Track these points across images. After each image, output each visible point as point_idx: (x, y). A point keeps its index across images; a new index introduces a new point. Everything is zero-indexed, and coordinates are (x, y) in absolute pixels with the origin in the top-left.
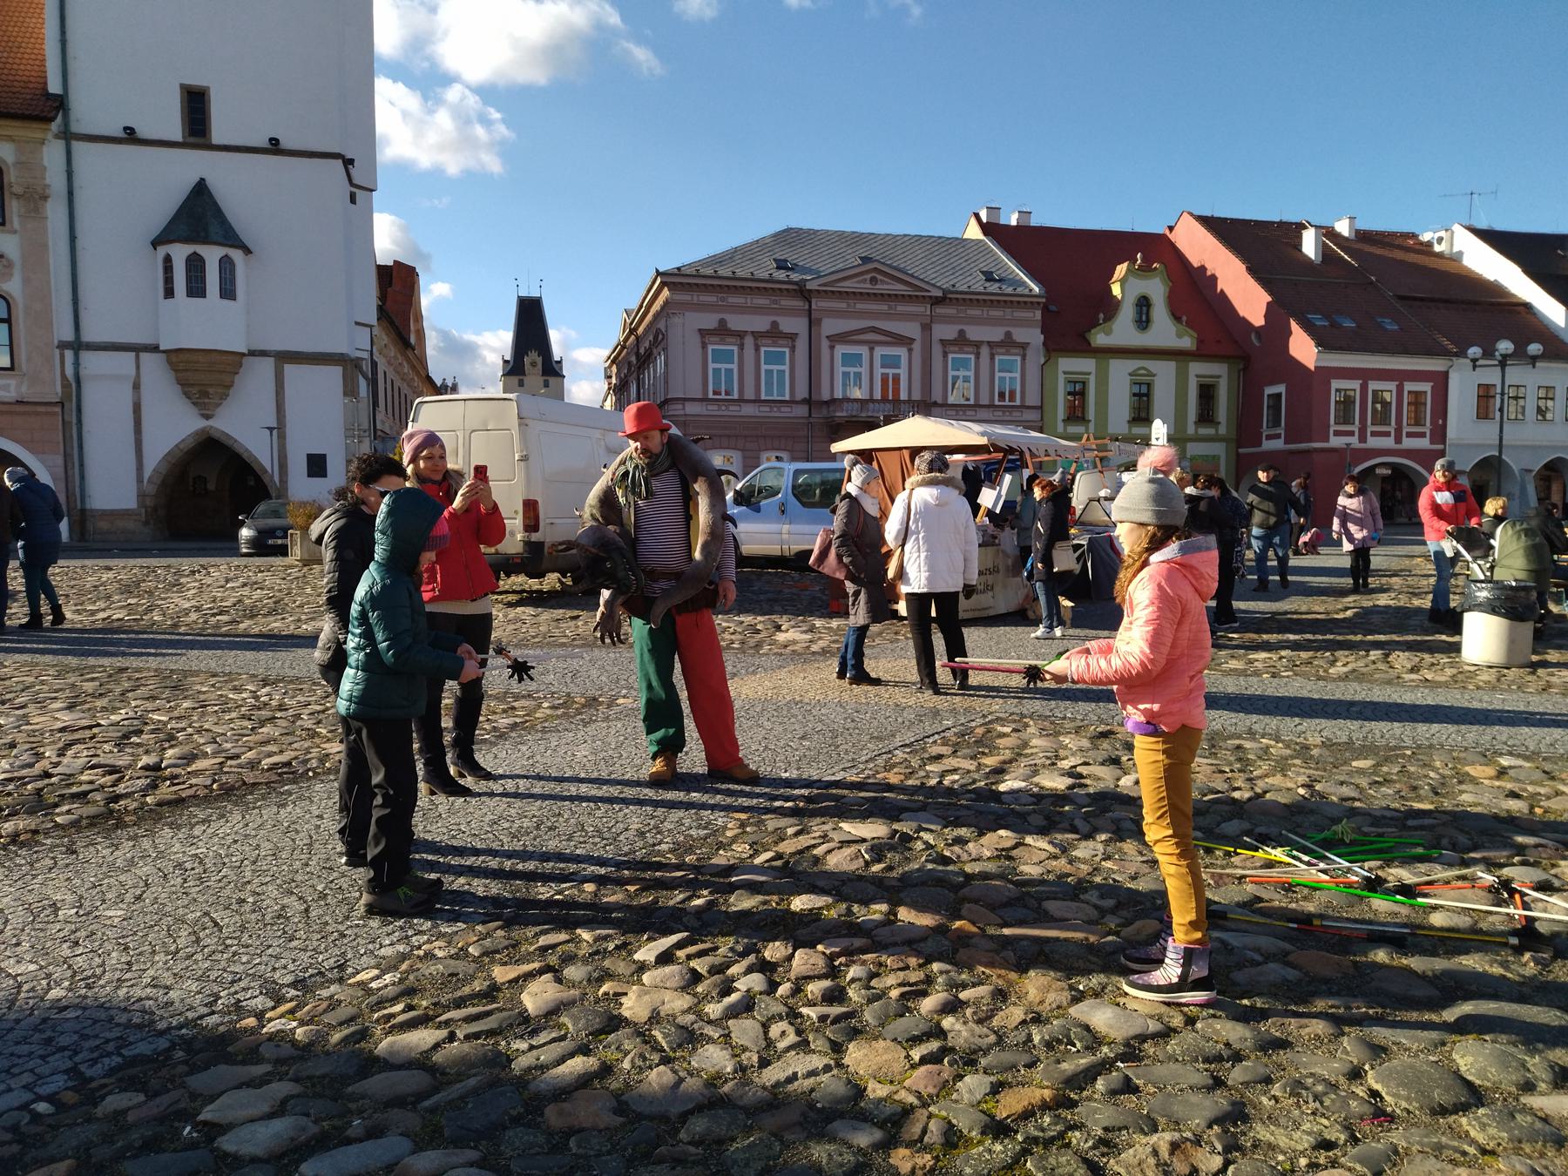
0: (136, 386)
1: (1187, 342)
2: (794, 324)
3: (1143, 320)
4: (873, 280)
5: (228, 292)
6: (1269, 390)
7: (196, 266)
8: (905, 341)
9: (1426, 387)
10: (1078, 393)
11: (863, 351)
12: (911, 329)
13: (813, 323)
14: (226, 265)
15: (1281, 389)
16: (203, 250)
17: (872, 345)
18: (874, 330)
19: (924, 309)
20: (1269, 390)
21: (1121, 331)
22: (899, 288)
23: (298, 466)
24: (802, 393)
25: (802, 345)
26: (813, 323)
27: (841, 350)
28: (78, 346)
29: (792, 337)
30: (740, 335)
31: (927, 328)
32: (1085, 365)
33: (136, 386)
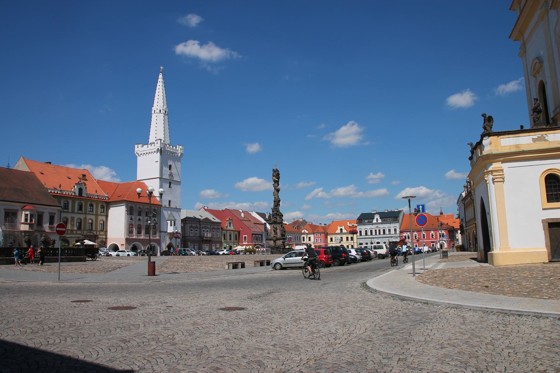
2: (198, 226)
6: (244, 236)
9: (261, 236)
12: (209, 226)
13: (200, 226)
15: (246, 236)
17: (206, 229)
19: (210, 224)
20: (244, 236)
24: (199, 236)
25: (199, 228)
26: (200, 226)
27: (203, 229)
29: (198, 228)
30: (193, 227)
31: (211, 226)
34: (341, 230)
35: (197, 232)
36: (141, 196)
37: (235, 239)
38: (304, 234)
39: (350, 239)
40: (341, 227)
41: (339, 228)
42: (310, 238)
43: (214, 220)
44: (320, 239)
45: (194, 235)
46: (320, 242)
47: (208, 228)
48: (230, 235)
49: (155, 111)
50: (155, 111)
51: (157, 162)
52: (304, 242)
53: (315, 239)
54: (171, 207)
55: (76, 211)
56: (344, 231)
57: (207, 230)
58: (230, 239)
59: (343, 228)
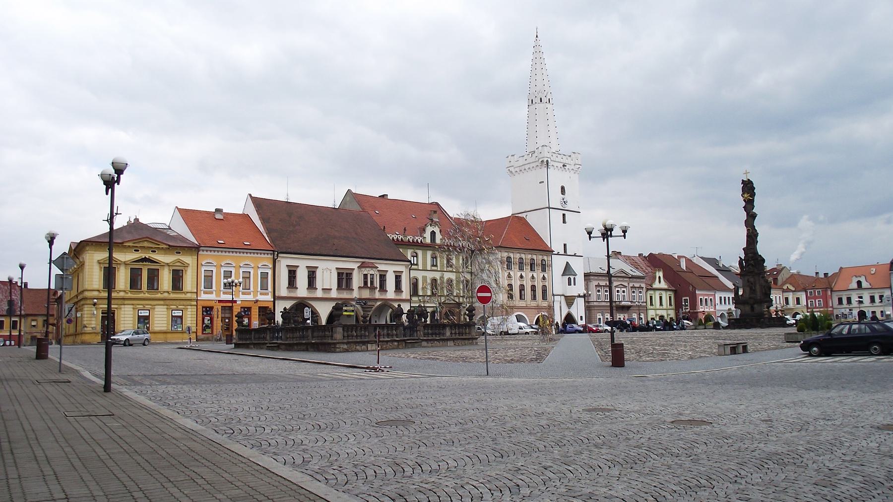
0: (560, 303)
1: (666, 287)
3: (660, 282)
4: (621, 273)
5: (575, 284)
7: (569, 279)
8: (625, 287)
10: (651, 297)
11: (619, 289)
12: (626, 284)
14: (574, 279)
16: (570, 276)
18: (621, 285)
21: (656, 285)
22: (624, 275)
23: (579, 318)
27: (617, 289)
28: (553, 295)
31: (628, 284)
32: (652, 292)
33: (560, 303)
34: (859, 283)
35: (635, 294)
36: (594, 237)
37: (669, 304)
38: (788, 290)
39: (877, 299)
40: (859, 279)
41: (855, 280)
42: (798, 299)
43: (634, 274)
44: (818, 301)
45: (603, 299)
46: (817, 305)
47: (625, 287)
48: (661, 298)
49: (532, 100)
50: (532, 100)
51: (543, 182)
52: (788, 306)
53: (809, 301)
54: (568, 254)
55: (429, 268)
56: (865, 284)
57: (623, 289)
58: (661, 304)
59: (862, 279)
